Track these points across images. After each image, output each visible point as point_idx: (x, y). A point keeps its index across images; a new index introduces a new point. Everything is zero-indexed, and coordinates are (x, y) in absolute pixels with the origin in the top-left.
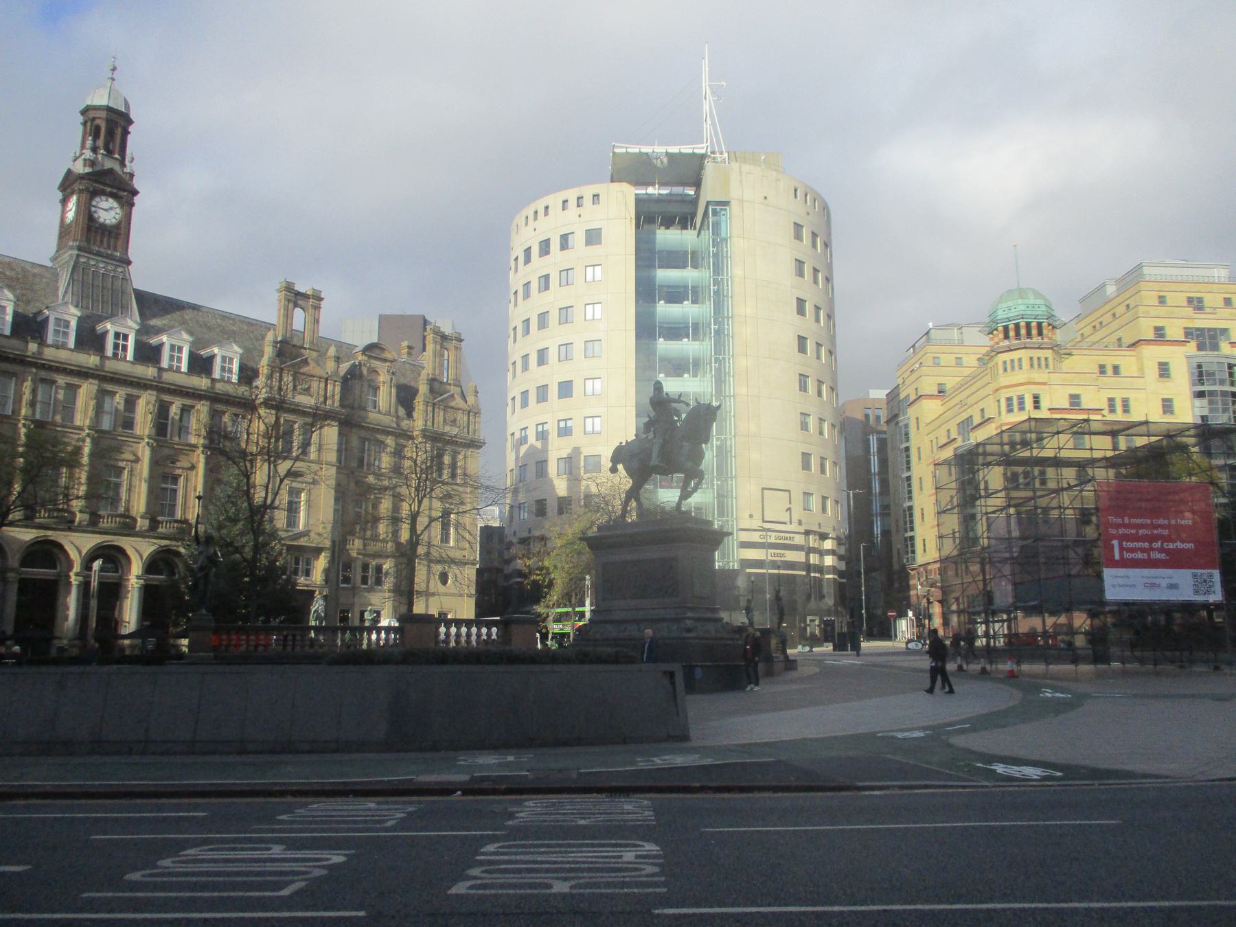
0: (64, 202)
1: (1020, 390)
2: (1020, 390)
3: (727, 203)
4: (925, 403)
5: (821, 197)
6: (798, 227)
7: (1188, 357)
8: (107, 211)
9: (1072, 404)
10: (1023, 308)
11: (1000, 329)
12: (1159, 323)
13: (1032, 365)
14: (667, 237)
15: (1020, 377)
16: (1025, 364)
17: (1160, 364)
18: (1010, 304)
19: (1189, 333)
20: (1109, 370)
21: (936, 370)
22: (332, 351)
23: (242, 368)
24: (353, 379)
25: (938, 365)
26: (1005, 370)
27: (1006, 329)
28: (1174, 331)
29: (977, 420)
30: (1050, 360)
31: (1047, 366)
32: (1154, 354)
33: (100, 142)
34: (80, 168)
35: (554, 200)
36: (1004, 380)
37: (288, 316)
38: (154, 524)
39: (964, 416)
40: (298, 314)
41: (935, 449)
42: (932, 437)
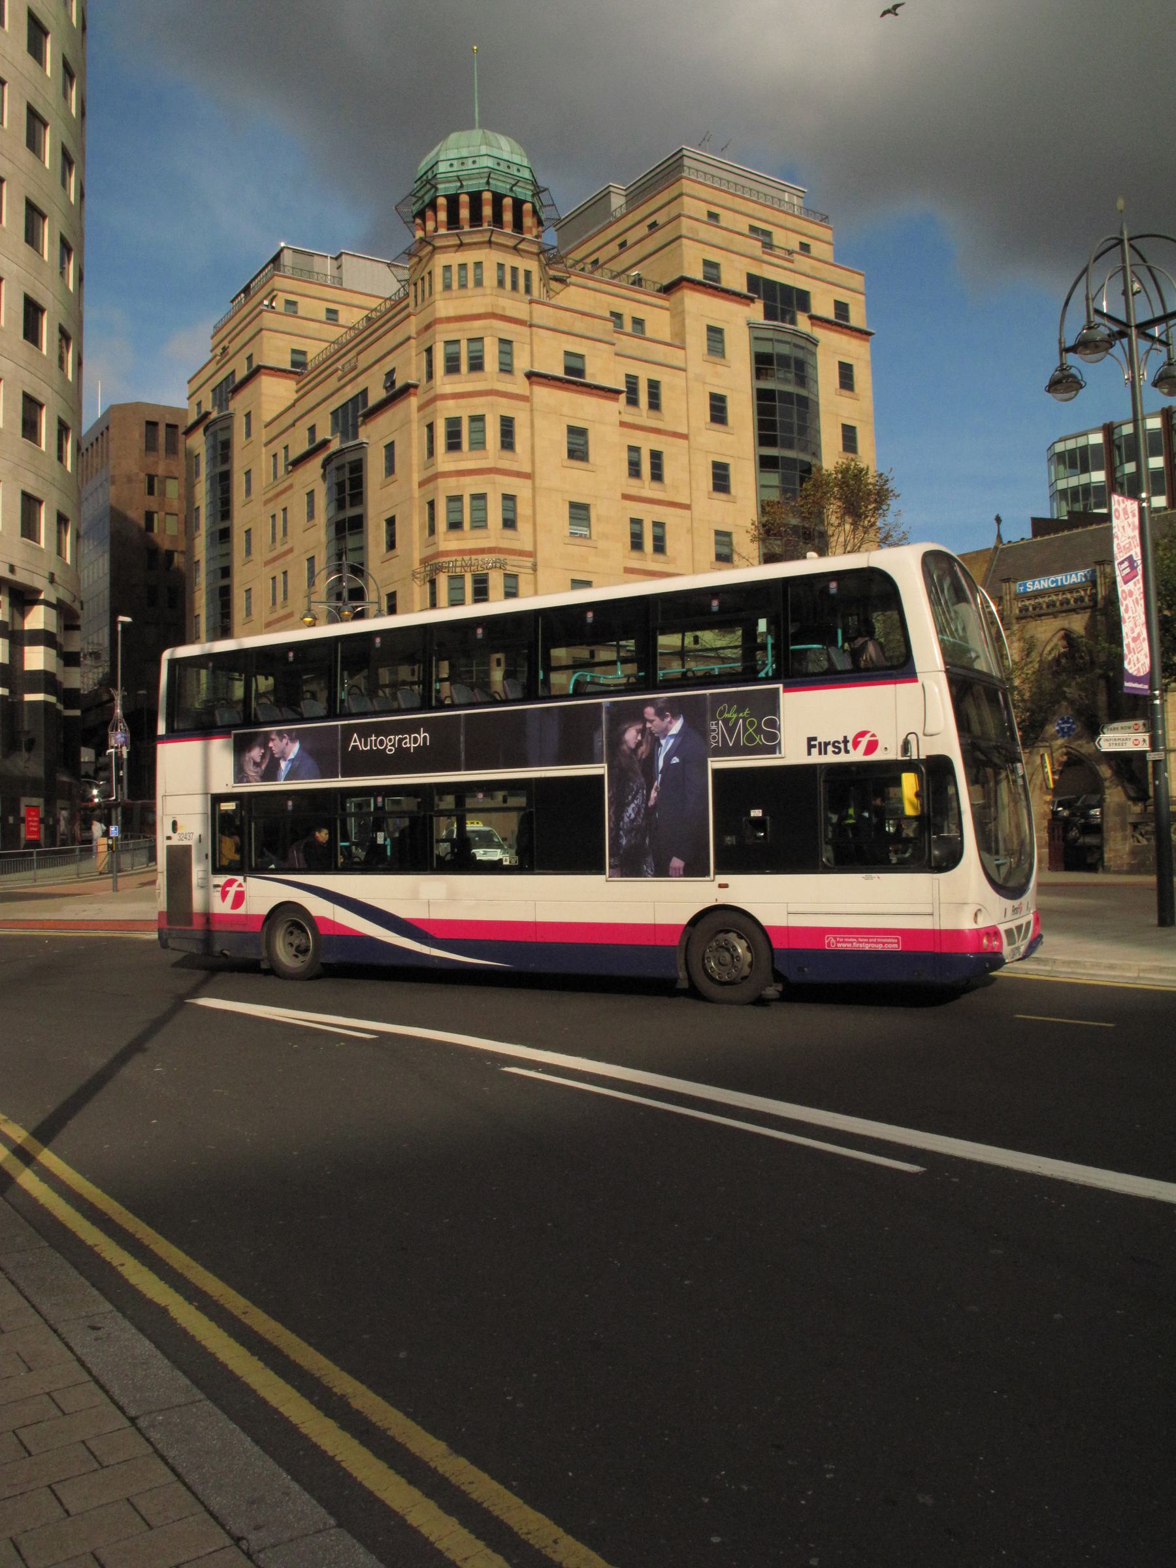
1: (476, 328)
2: (476, 328)
4: (267, 383)
7: (752, 326)
9: (569, 370)
10: (490, 163)
11: (442, 201)
12: (714, 256)
13: (501, 283)
15: (476, 302)
16: (490, 276)
17: (712, 330)
18: (464, 153)
19: (754, 282)
20: (628, 326)
21: (289, 323)
25: (295, 314)
26: (447, 287)
27: (453, 202)
28: (734, 279)
29: (377, 394)
30: (535, 278)
31: (528, 290)
32: (700, 308)
36: (444, 307)
39: (350, 392)
41: (281, 470)
42: (277, 447)
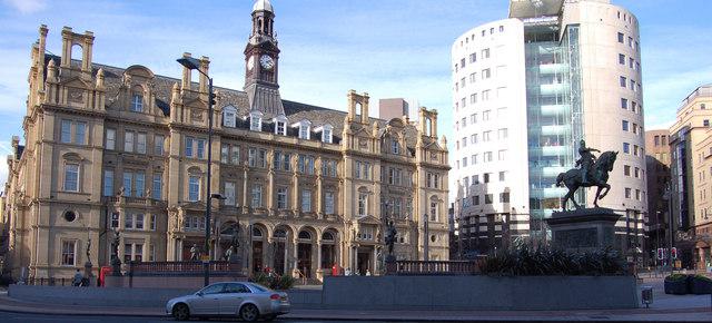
0: (247, 59)
3: (578, 25)
5: (634, 17)
6: (620, 35)
8: (267, 62)
14: (542, 49)
22: (375, 124)
23: (334, 137)
24: (386, 139)
33: (262, 29)
34: (254, 42)
35: (477, 31)
37: (354, 108)
38: (276, 213)
40: (358, 106)
